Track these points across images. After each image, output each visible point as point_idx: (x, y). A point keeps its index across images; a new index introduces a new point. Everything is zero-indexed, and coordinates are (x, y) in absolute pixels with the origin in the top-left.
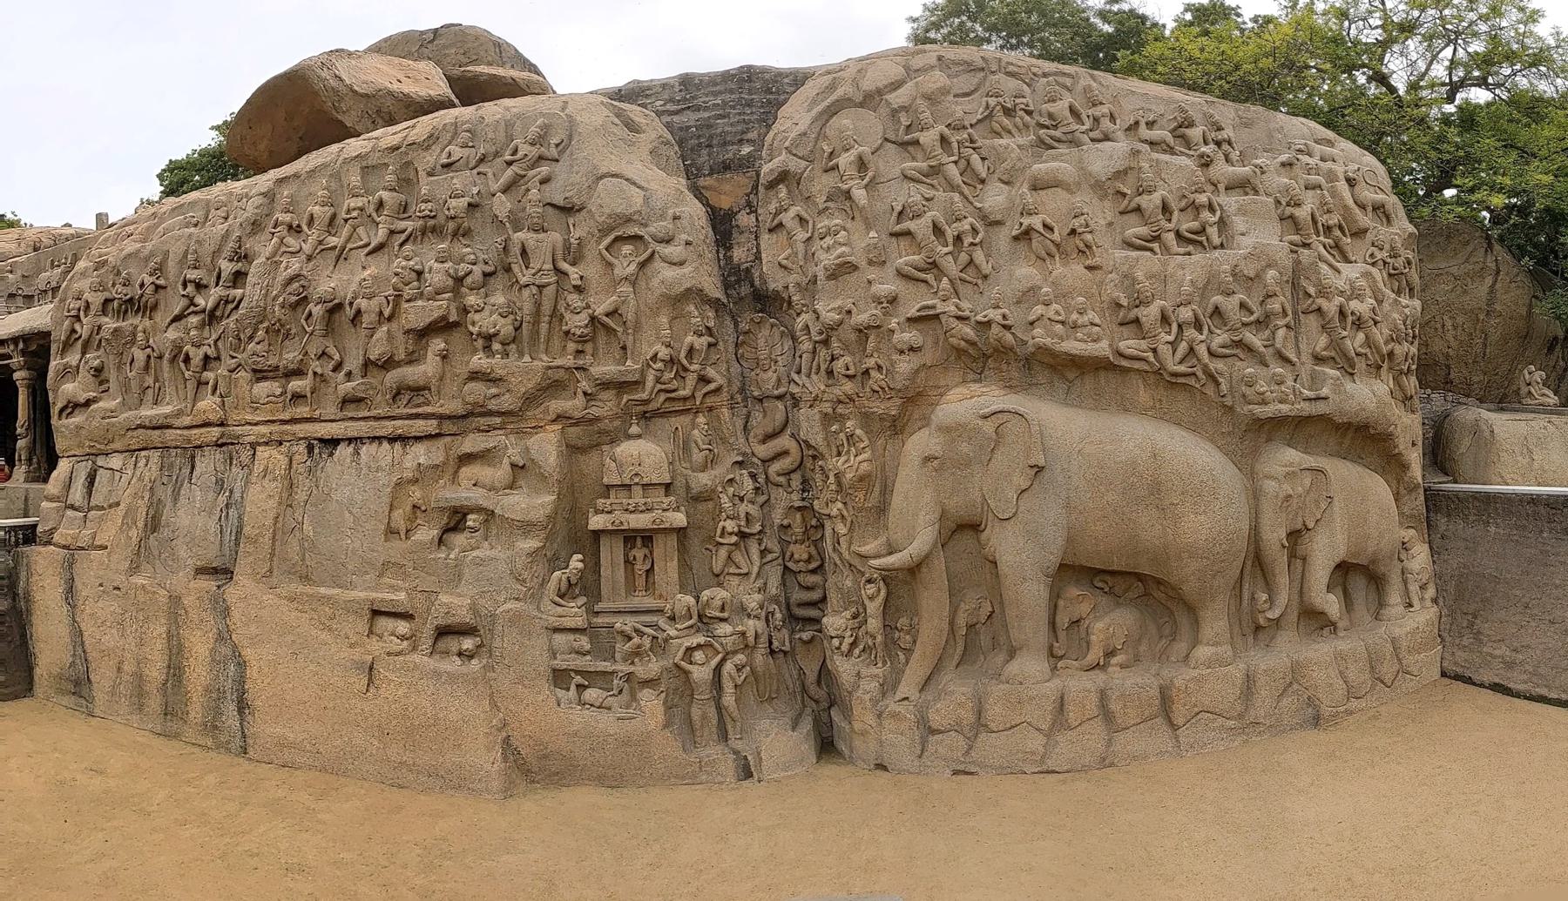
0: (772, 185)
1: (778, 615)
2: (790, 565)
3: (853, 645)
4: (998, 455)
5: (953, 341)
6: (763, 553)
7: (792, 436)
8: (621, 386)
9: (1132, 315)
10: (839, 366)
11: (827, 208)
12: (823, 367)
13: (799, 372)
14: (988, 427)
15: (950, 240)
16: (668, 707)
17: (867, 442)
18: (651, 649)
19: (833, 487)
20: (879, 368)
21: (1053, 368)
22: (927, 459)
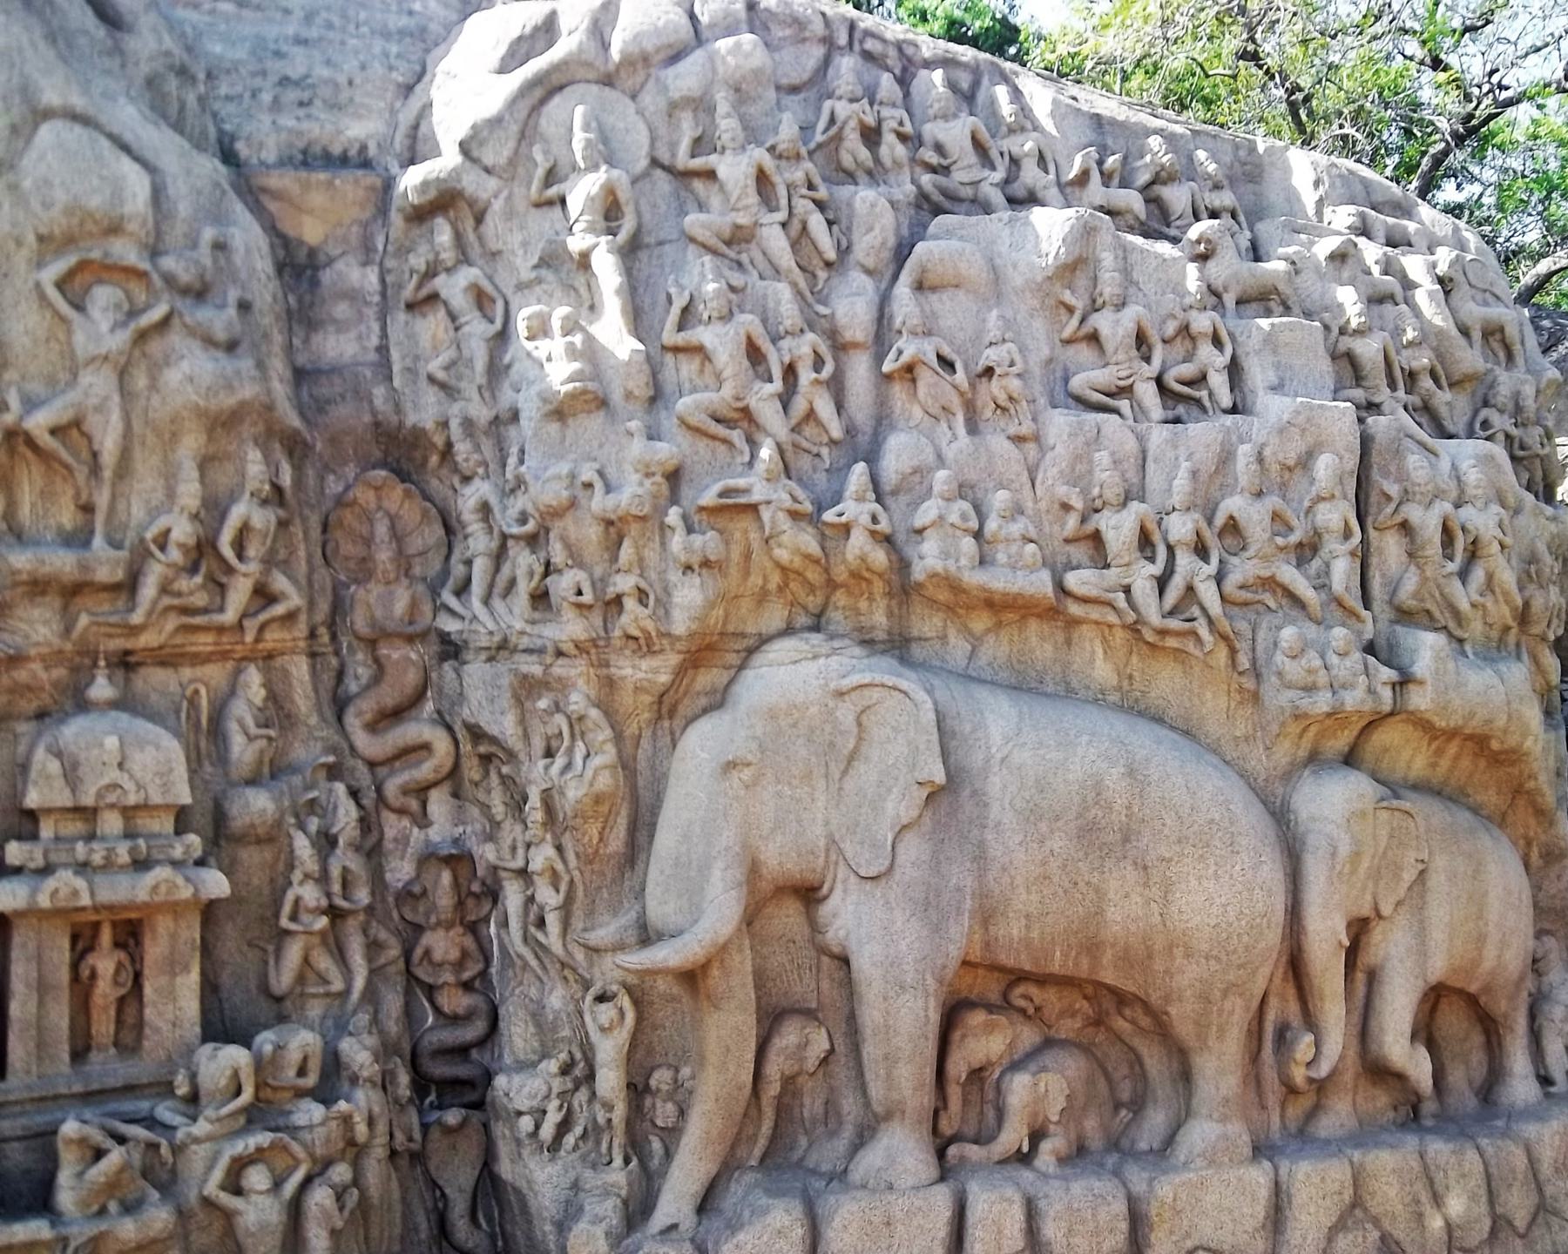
0: (420, 215)
2: (420, 973)
4: (860, 767)
5: (782, 555)
6: (373, 947)
7: (439, 712)
8: (74, 591)
9: (1089, 528)
10: (562, 585)
11: (539, 281)
14: (846, 714)
15: (777, 373)
19: (538, 816)
20: (642, 596)
21: (949, 609)
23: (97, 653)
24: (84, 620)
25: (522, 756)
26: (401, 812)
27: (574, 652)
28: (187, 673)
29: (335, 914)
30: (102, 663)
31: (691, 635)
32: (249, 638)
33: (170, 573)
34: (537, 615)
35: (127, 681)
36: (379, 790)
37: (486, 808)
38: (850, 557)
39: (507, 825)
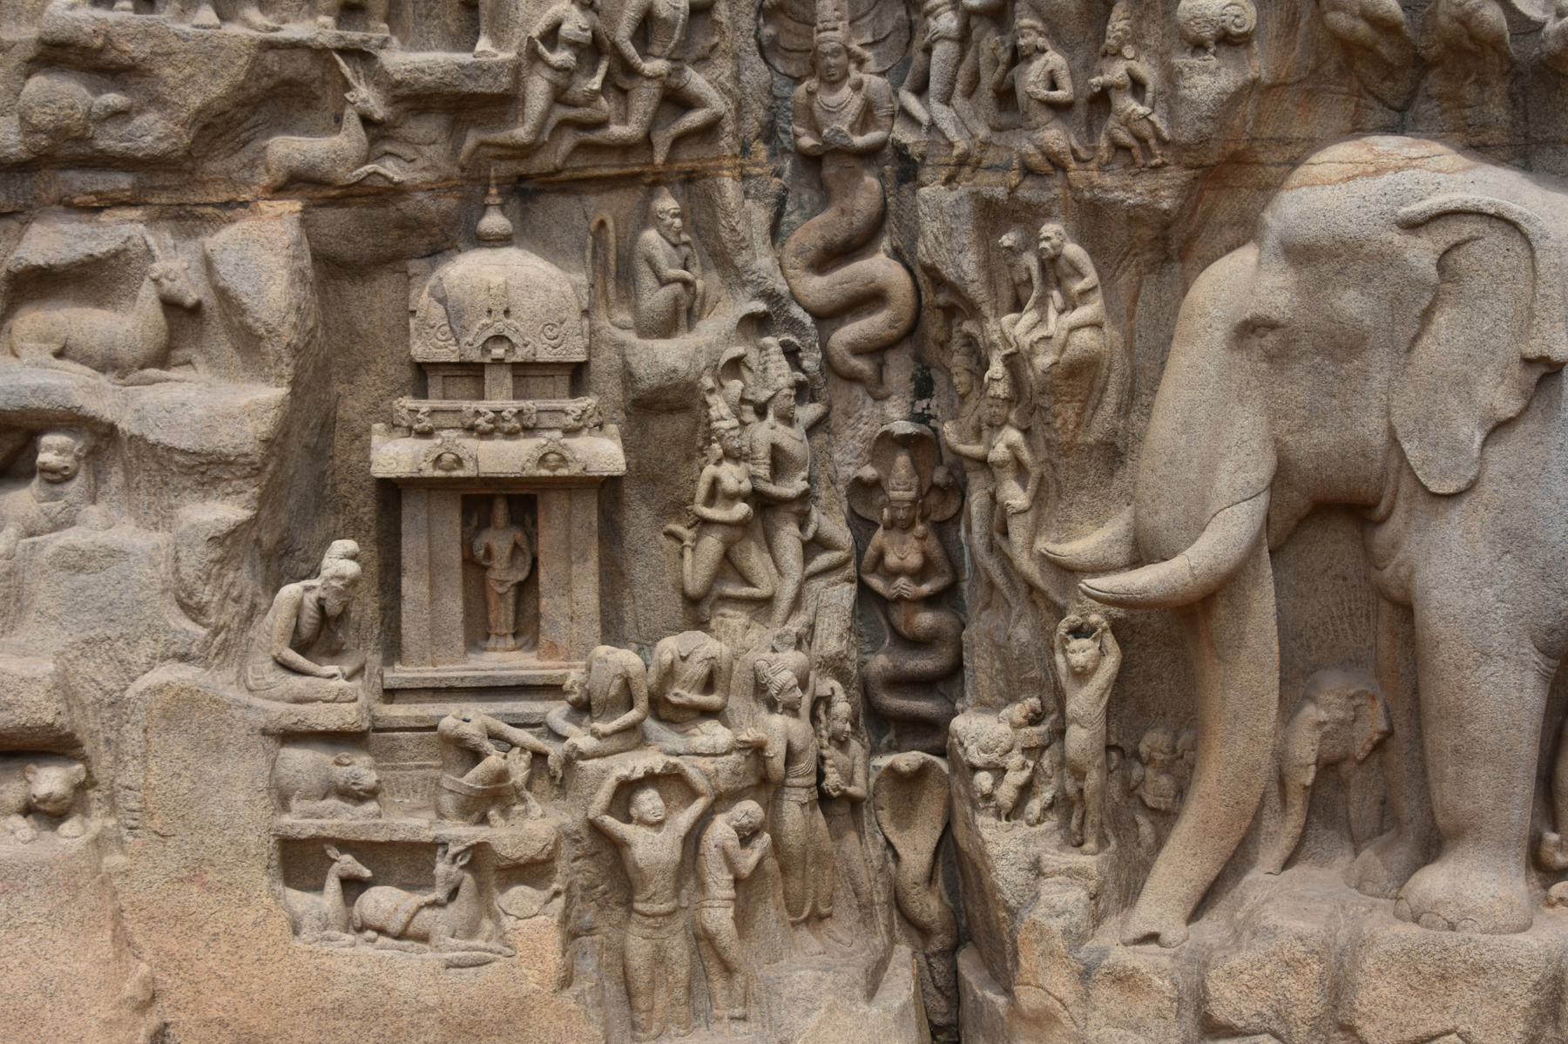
1: (842, 707)
2: (876, 583)
3: (1026, 790)
5: (1341, 21)
8: (458, 105)
10: (1032, 78)
12: (988, 79)
13: (921, 89)
14: (1421, 253)
16: (572, 934)
17: (1091, 278)
18: (529, 785)
19: (1001, 389)
20: (1137, 86)
22: (1249, 330)
23: (488, 178)
24: (471, 140)
25: (986, 309)
26: (853, 378)
27: (1048, 168)
28: (592, 200)
29: (763, 503)
30: (493, 191)
31: (1204, 141)
32: (659, 159)
33: (560, 79)
34: (1005, 119)
35: (525, 212)
36: (824, 349)
37: (950, 376)
38: (1443, 20)
39: (973, 403)
